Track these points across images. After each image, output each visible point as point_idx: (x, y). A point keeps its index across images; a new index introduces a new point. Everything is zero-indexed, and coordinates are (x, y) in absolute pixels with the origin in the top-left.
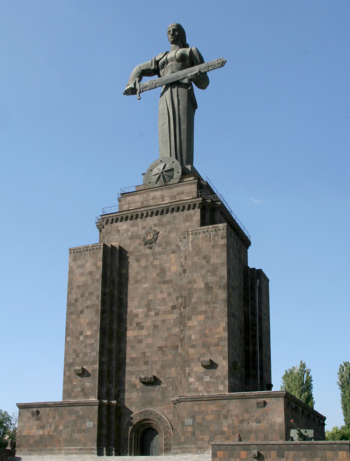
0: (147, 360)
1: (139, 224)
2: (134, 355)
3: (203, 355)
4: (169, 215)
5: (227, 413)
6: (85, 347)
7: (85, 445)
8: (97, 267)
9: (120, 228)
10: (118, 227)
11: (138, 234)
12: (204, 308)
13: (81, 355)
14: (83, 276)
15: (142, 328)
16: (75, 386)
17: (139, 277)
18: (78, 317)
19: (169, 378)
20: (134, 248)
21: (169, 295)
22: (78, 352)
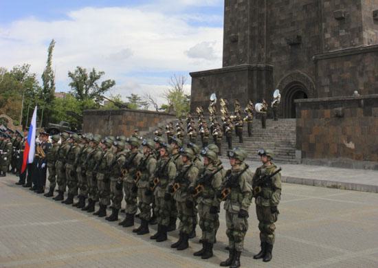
2: (283, 18)
5: (363, 70)
13: (236, 23)
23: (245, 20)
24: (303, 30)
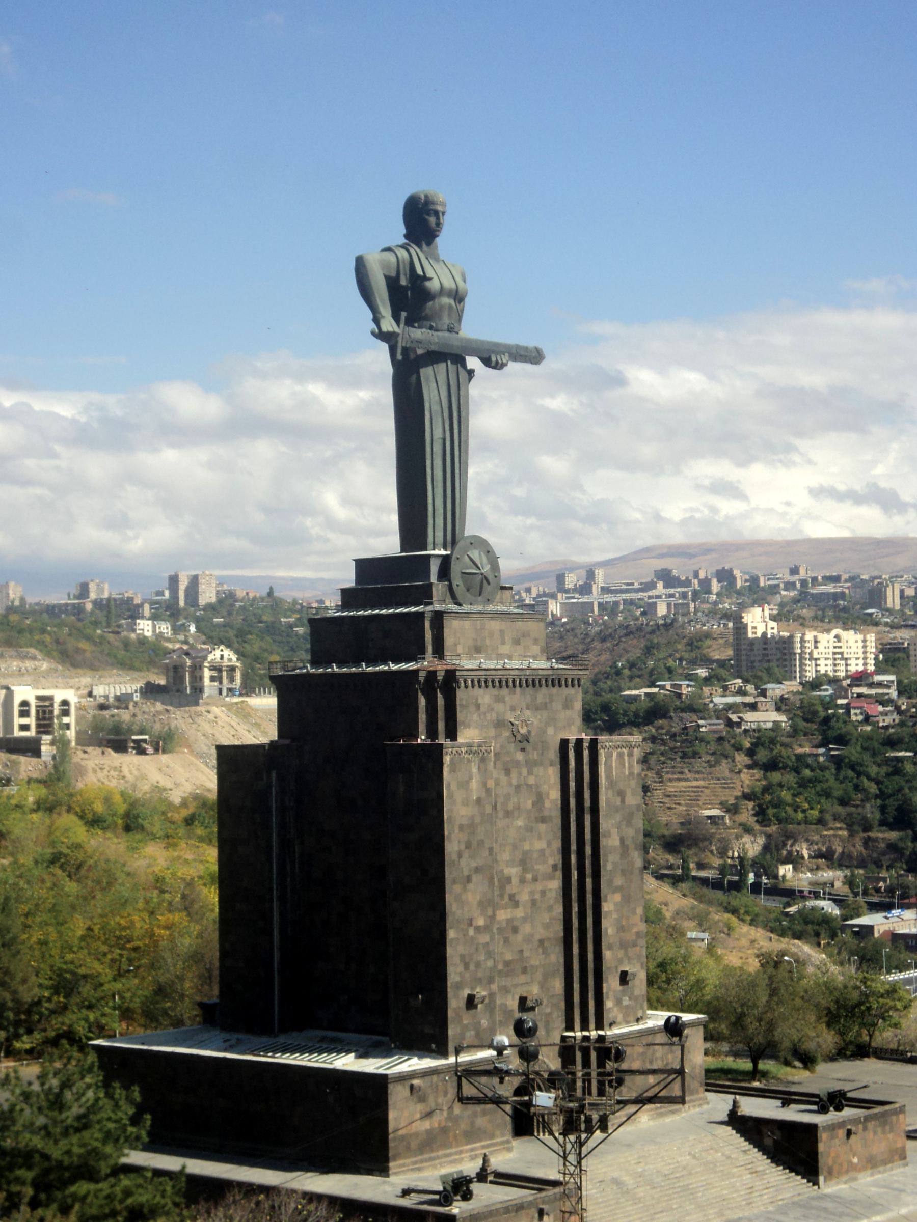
0: (525, 964)
1: (507, 699)
2: (509, 957)
3: (620, 961)
4: (544, 689)
6: (477, 950)
7: (492, 1136)
8: (488, 791)
9: (480, 701)
10: (477, 700)
11: (506, 718)
12: (619, 881)
13: (472, 967)
14: (467, 805)
15: (516, 904)
16: (465, 1028)
17: (510, 808)
18: (465, 889)
19: (553, 996)
20: (502, 747)
21: (549, 844)
22: (467, 960)
23: (490, 963)
24: (539, 982)
